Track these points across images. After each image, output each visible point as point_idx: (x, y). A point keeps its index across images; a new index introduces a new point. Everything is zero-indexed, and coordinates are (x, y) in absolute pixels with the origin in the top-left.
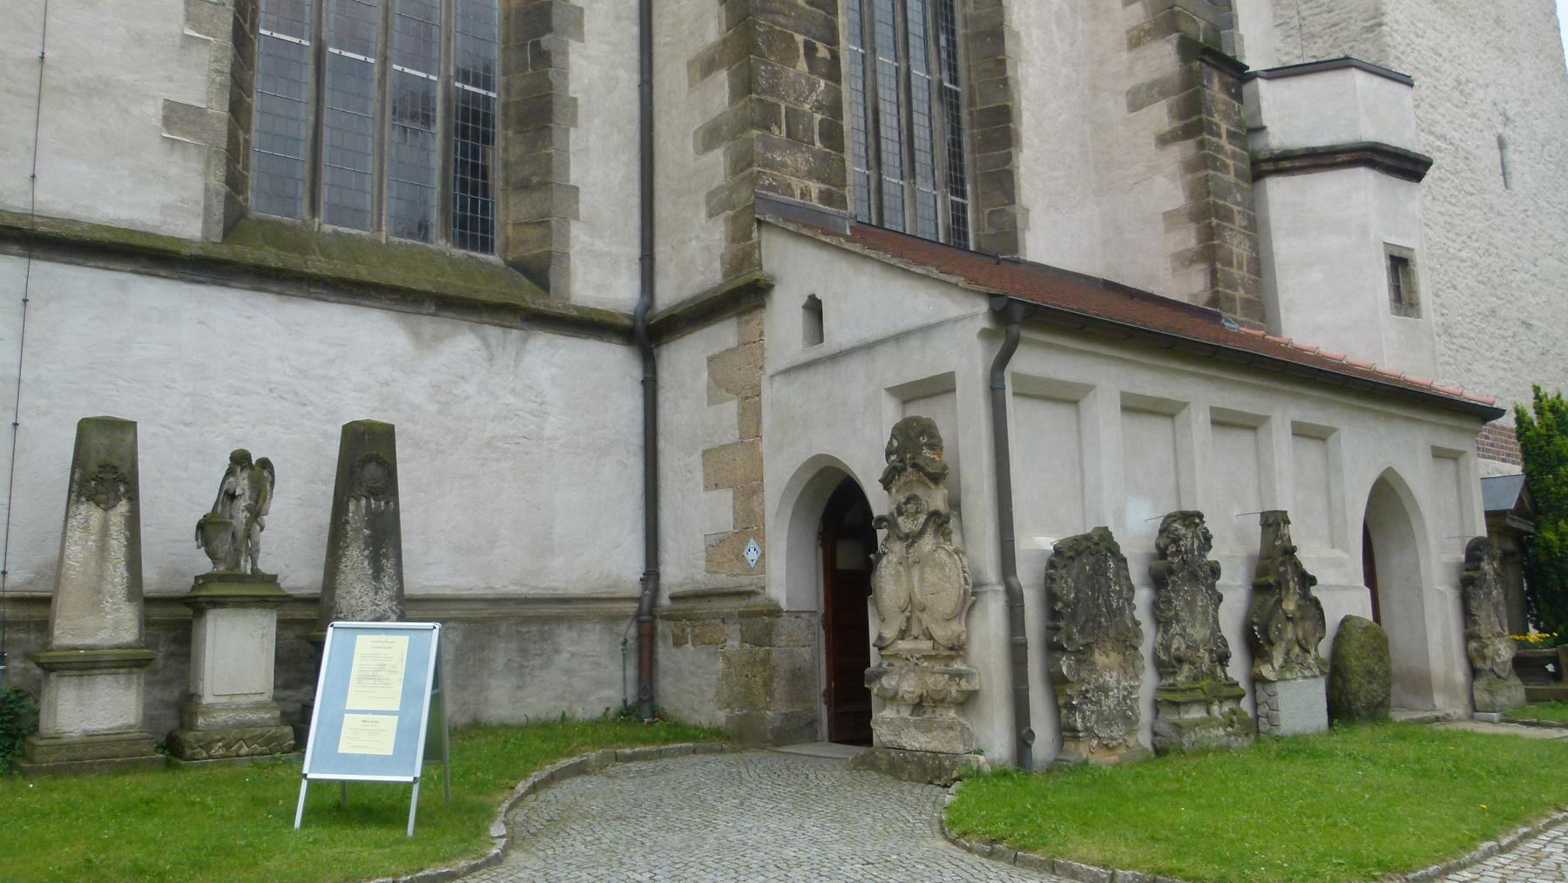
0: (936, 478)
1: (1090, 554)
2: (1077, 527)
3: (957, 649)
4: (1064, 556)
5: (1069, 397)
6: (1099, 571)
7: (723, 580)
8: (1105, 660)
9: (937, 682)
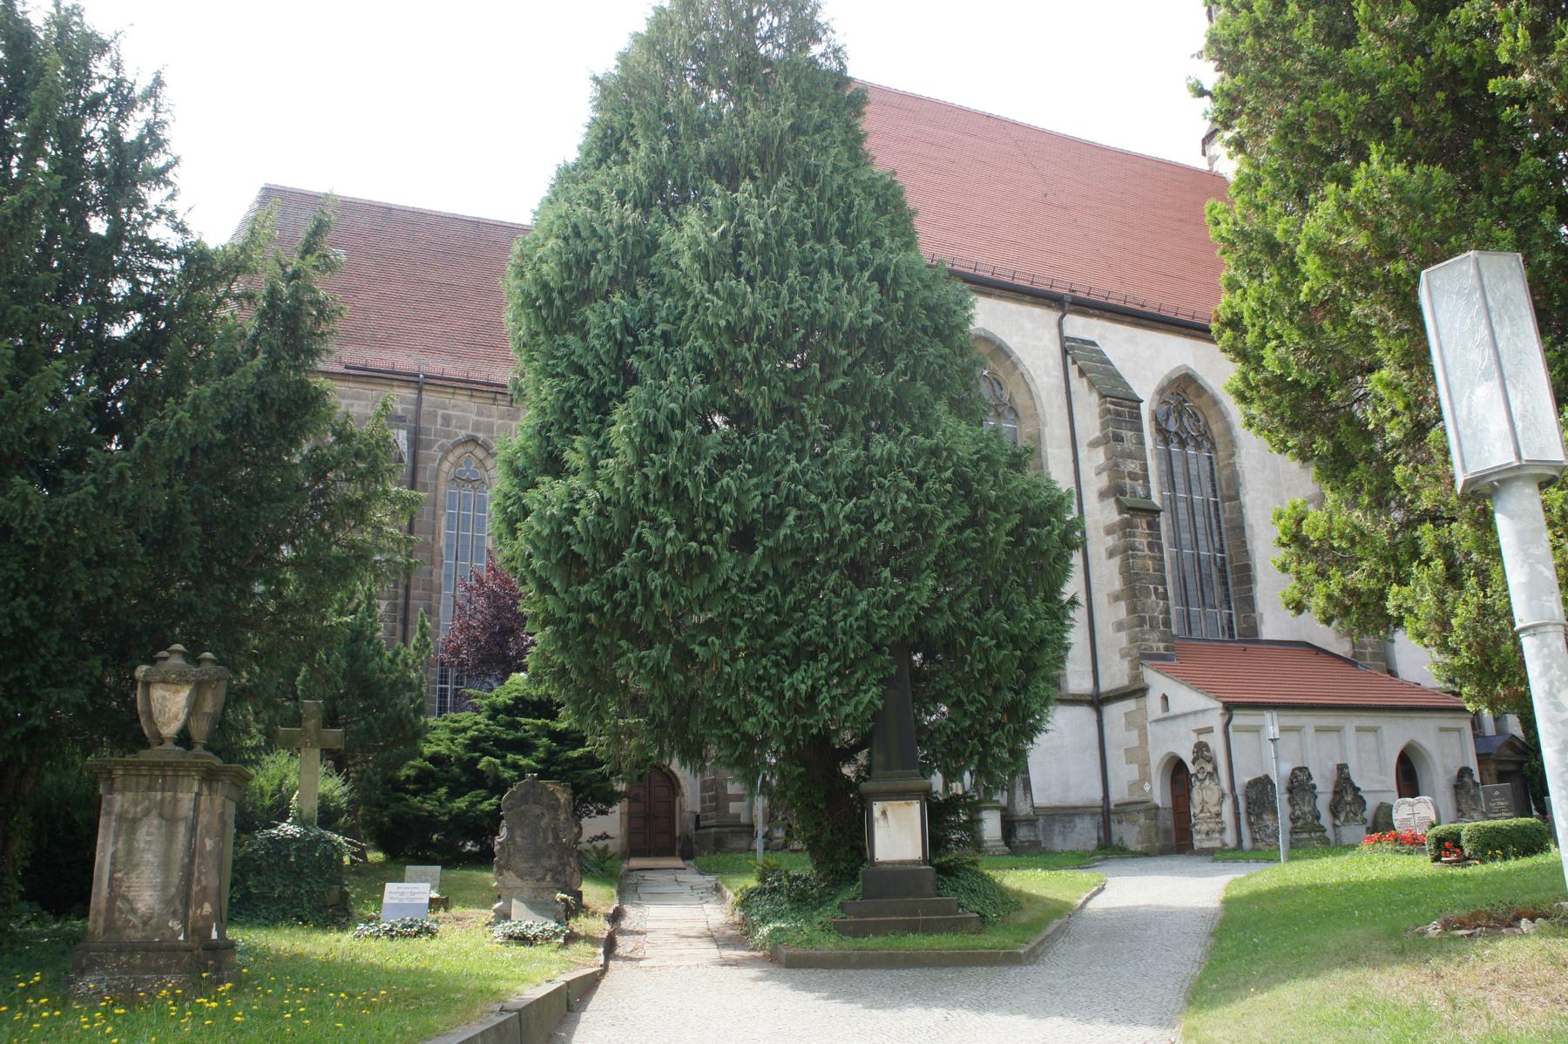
1: (1261, 786)
2: (1260, 774)
3: (1218, 815)
4: (1252, 784)
7: (1136, 798)
9: (1212, 826)
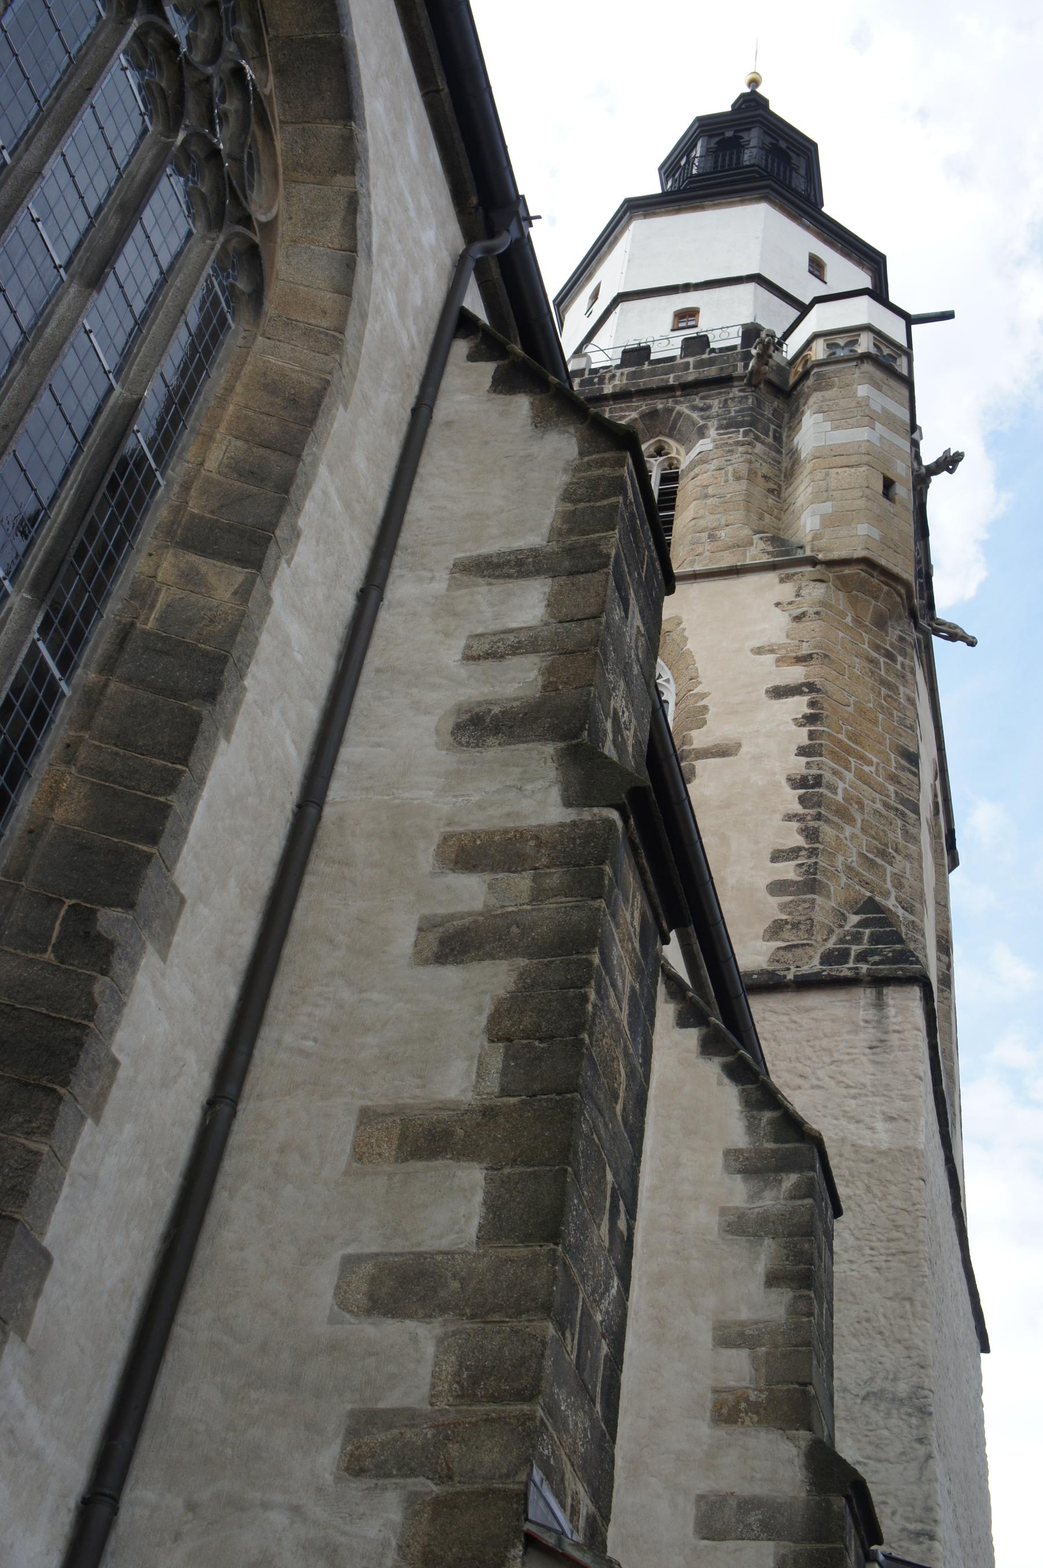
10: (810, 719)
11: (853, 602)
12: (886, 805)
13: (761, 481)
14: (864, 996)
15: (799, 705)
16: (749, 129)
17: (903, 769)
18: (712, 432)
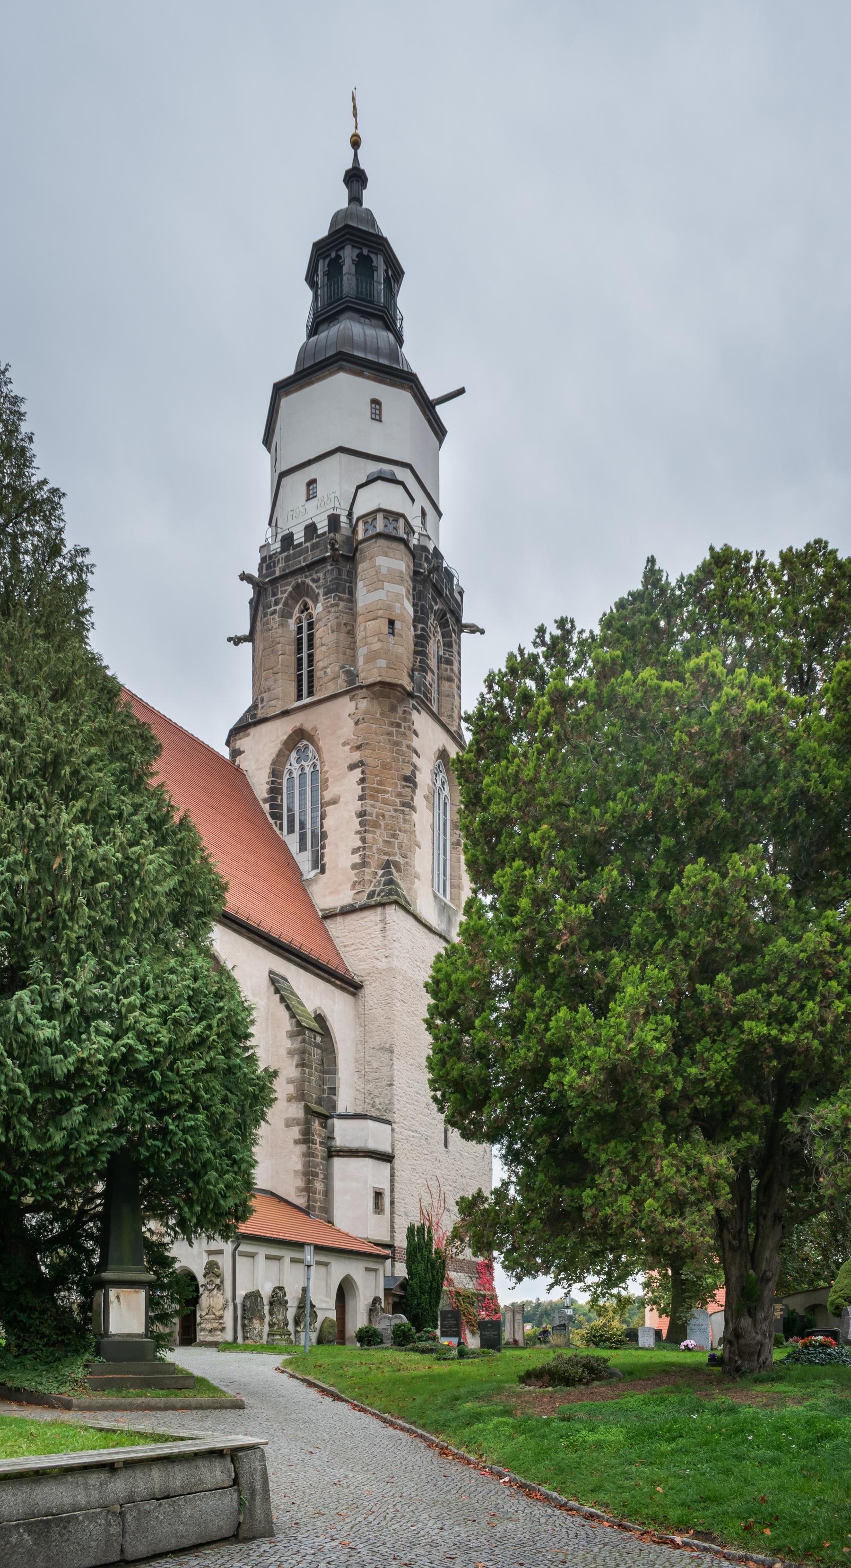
0: (218, 1276)
1: (254, 1297)
2: (251, 1289)
3: (221, 1317)
4: (247, 1297)
5: (252, 1256)
6: (256, 1300)
8: (256, 1323)
9: (216, 1325)
10: (362, 781)
11: (380, 703)
12: (396, 811)
13: (343, 627)
14: (379, 910)
15: (357, 773)
16: (343, 248)
17: (404, 787)
18: (321, 598)
